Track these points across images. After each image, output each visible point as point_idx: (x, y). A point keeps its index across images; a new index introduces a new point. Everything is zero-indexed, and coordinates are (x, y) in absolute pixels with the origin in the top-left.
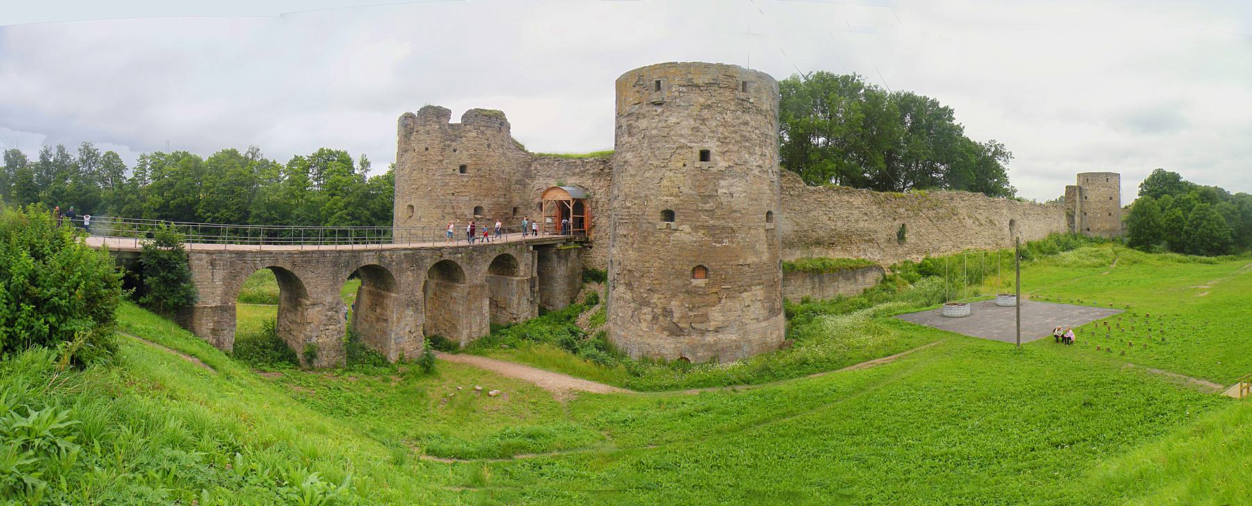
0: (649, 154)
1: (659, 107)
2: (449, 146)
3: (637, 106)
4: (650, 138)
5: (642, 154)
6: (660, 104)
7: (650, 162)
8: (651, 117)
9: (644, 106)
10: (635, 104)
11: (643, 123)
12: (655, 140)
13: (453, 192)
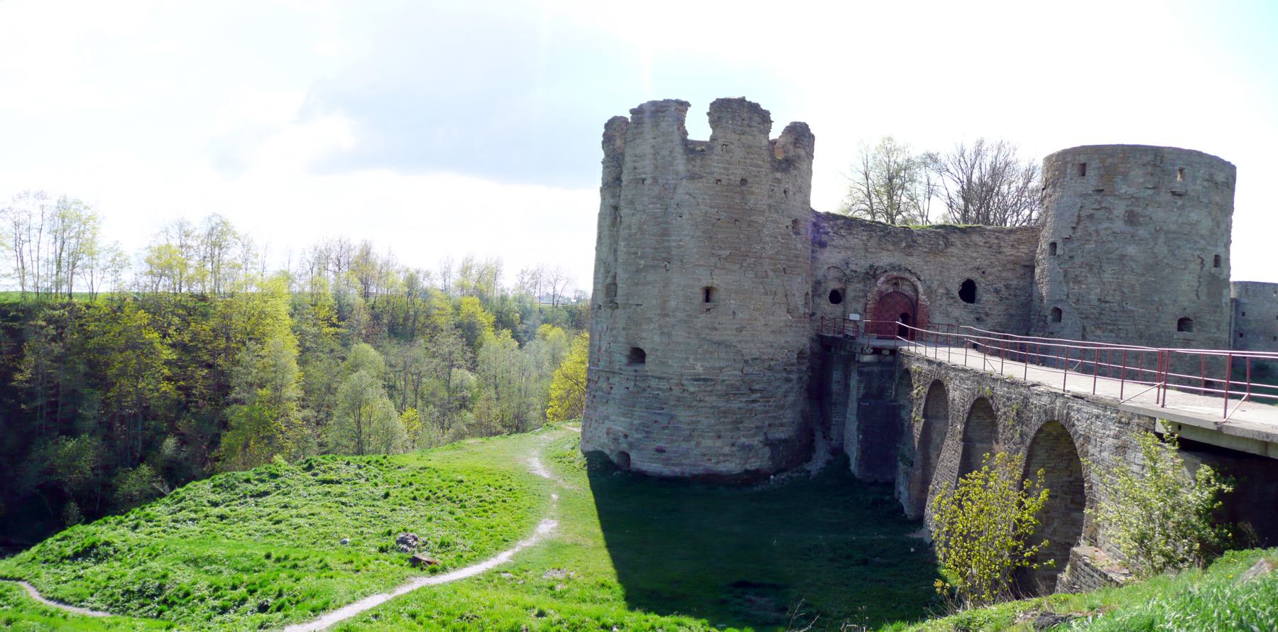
0: (1166, 252)
1: (1177, 197)
2: (779, 181)
3: (1150, 192)
4: (1167, 232)
5: (1155, 250)
6: (1180, 195)
7: (1166, 261)
8: (1170, 208)
9: (1162, 194)
10: (1146, 188)
11: (1159, 214)
12: (1174, 236)
13: (785, 266)
